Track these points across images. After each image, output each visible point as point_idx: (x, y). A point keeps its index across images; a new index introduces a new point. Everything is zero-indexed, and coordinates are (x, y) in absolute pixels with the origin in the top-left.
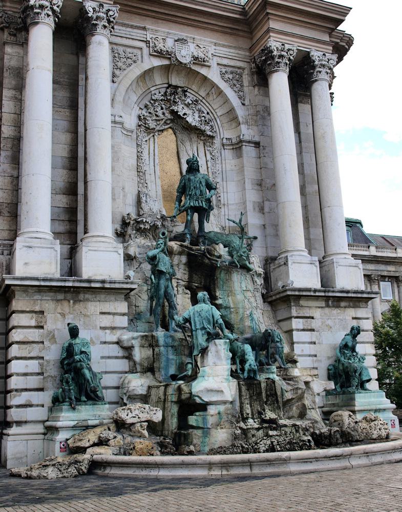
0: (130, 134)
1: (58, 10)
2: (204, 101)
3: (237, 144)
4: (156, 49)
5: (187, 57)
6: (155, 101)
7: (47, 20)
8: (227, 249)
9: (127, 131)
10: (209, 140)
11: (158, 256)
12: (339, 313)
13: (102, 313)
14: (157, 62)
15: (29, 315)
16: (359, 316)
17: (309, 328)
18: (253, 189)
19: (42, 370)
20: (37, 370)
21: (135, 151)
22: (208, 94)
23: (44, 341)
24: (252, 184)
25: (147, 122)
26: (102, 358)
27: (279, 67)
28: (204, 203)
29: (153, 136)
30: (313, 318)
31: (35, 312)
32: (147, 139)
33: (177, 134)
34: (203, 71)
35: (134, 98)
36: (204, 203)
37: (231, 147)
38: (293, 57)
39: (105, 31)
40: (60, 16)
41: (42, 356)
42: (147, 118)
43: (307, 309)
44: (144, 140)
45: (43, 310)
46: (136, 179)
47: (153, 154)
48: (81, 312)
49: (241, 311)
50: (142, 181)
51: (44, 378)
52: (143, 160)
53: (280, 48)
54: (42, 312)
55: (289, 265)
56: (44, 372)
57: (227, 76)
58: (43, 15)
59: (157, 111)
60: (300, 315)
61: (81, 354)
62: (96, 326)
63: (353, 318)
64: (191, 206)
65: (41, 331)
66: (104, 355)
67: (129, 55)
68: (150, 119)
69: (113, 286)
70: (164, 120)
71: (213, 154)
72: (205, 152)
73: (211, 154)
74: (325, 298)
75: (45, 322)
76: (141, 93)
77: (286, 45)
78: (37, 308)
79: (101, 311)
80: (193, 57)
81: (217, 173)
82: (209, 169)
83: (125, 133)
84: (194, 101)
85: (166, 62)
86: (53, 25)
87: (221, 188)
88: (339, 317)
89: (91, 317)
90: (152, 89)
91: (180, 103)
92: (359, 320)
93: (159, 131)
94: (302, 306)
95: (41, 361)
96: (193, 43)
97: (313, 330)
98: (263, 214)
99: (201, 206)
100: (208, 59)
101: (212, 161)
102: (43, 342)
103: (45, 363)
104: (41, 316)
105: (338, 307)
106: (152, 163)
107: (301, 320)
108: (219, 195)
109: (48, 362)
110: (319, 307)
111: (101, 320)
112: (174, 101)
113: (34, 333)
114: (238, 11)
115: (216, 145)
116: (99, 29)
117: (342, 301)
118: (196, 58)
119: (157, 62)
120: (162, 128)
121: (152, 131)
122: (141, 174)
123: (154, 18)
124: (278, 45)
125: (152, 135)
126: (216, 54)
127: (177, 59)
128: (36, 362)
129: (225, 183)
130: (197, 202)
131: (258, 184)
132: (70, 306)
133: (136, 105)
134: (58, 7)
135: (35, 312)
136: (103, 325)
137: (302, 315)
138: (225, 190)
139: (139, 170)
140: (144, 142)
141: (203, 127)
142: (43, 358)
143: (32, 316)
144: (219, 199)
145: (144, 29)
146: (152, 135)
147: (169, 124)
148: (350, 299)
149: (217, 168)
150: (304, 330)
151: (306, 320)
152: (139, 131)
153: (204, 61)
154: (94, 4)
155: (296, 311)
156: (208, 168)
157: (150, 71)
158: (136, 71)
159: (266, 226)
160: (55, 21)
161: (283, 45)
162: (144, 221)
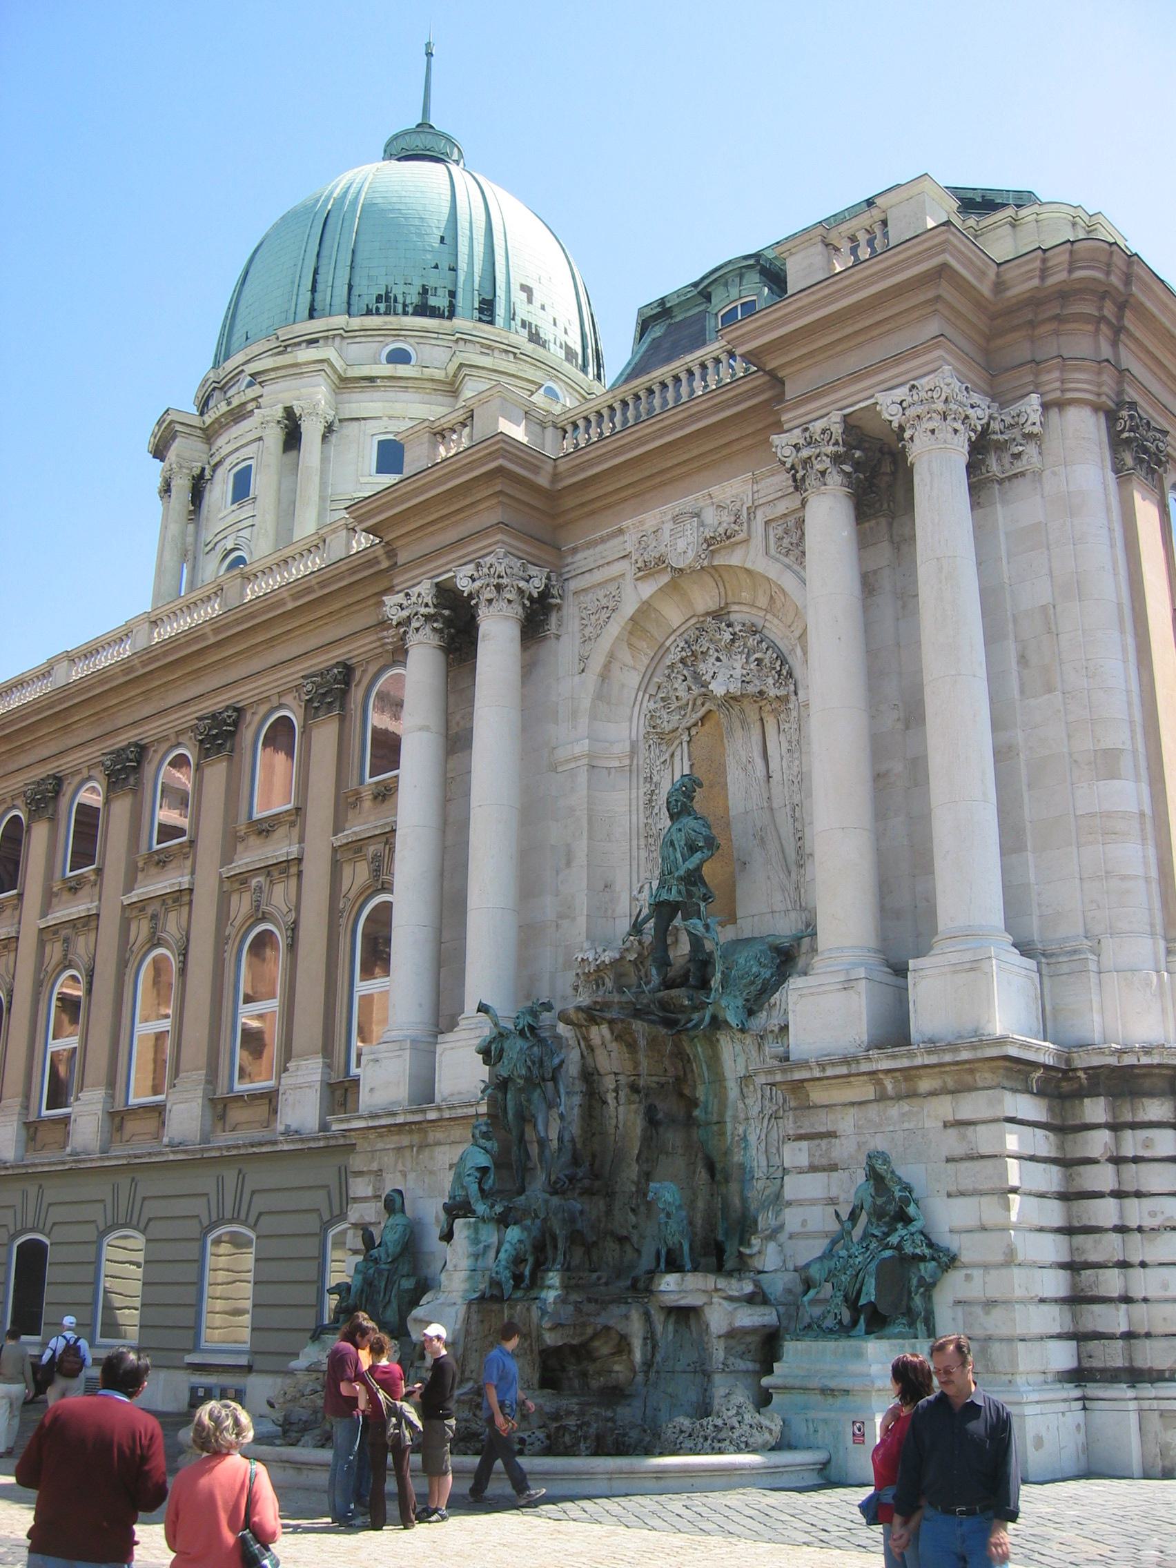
1: (431, 610)
2: (769, 617)
4: (638, 565)
5: (689, 551)
6: (672, 666)
7: (419, 637)
11: (493, 1048)
12: (904, 1115)
14: (648, 589)
16: (965, 1114)
17: (824, 1161)
22: (772, 596)
25: (659, 721)
27: (806, 490)
30: (831, 1135)
32: (667, 756)
34: (735, 559)
35: (633, 679)
38: (836, 443)
39: (491, 608)
40: (446, 612)
42: (658, 714)
43: (822, 1113)
44: (658, 763)
49: (729, 1127)
50: (655, 855)
52: (656, 810)
53: (802, 441)
57: (786, 542)
58: (411, 632)
59: (676, 689)
60: (802, 1131)
63: (946, 1125)
67: (604, 602)
68: (664, 713)
69: (454, 1114)
70: (691, 703)
74: (865, 1078)
76: (646, 662)
77: (810, 426)
78: (375, 1167)
80: (706, 540)
83: (617, 764)
84: (740, 631)
85: (665, 579)
86: (434, 640)
88: (906, 1126)
90: (668, 643)
91: (711, 652)
92: (962, 1129)
93: (689, 729)
94: (816, 1107)
96: (713, 504)
97: (833, 1168)
100: (737, 528)
105: (913, 1095)
107: (804, 1144)
108: (800, 835)
110: (853, 1104)
112: (702, 652)
114: (764, 383)
116: (483, 612)
117: (920, 1077)
118: (709, 542)
119: (648, 589)
120: (692, 721)
123: (636, 496)
124: (796, 436)
125: (677, 742)
126: (761, 501)
127: (672, 567)
133: (641, 694)
134: (427, 605)
137: (809, 1131)
141: (751, 689)
144: (799, 844)
145: (621, 531)
146: (677, 742)
147: (703, 705)
148: (937, 1070)
150: (813, 1169)
151: (817, 1142)
153: (728, 538)
154: (469, 569)
155: (795, 1122)
157: (646, 609)
158: (614, 629)
160: (434, 629)
161: (806, 430)
162: (579, 959)
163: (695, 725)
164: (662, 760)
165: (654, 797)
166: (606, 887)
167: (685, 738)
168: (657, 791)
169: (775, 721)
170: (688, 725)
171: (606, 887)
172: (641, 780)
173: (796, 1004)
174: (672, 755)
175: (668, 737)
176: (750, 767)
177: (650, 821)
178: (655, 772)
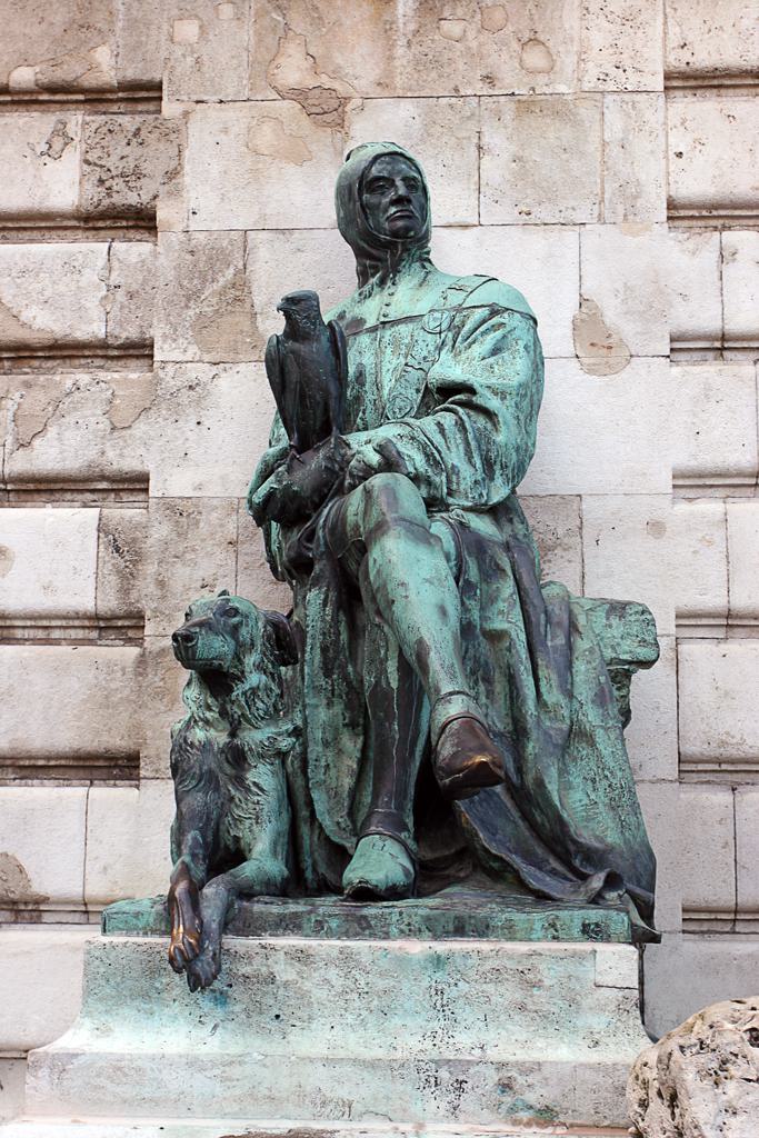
13: (691, 81)
15: (36, 125)
19: (125, 591)
20: (82, 592)
23: (156, 333)
26: (692, 482)
31: (96, 98)
41: (129, 464)
45: (157, 77)
48: (489, 79)
51: (142, 661)
54: (144, 93)
56: (148, 608)
61: (425, 409)
62: (631, 197)
65: (132, 250)
66: (709, 459)
75: (173, 174)
79: (678, 60)
89: (586, 112)
95: (125, 513)
102: (139, 350)
103: (160, 531)
104: (128, 122)
109: (181, 513)
111: (678, 142)
113: (72, 268)
128: (74, 521)
132: (388, 30)
135: (96, 98)
136: (696, 184)
142: (134, 484)
143: (61, 131)
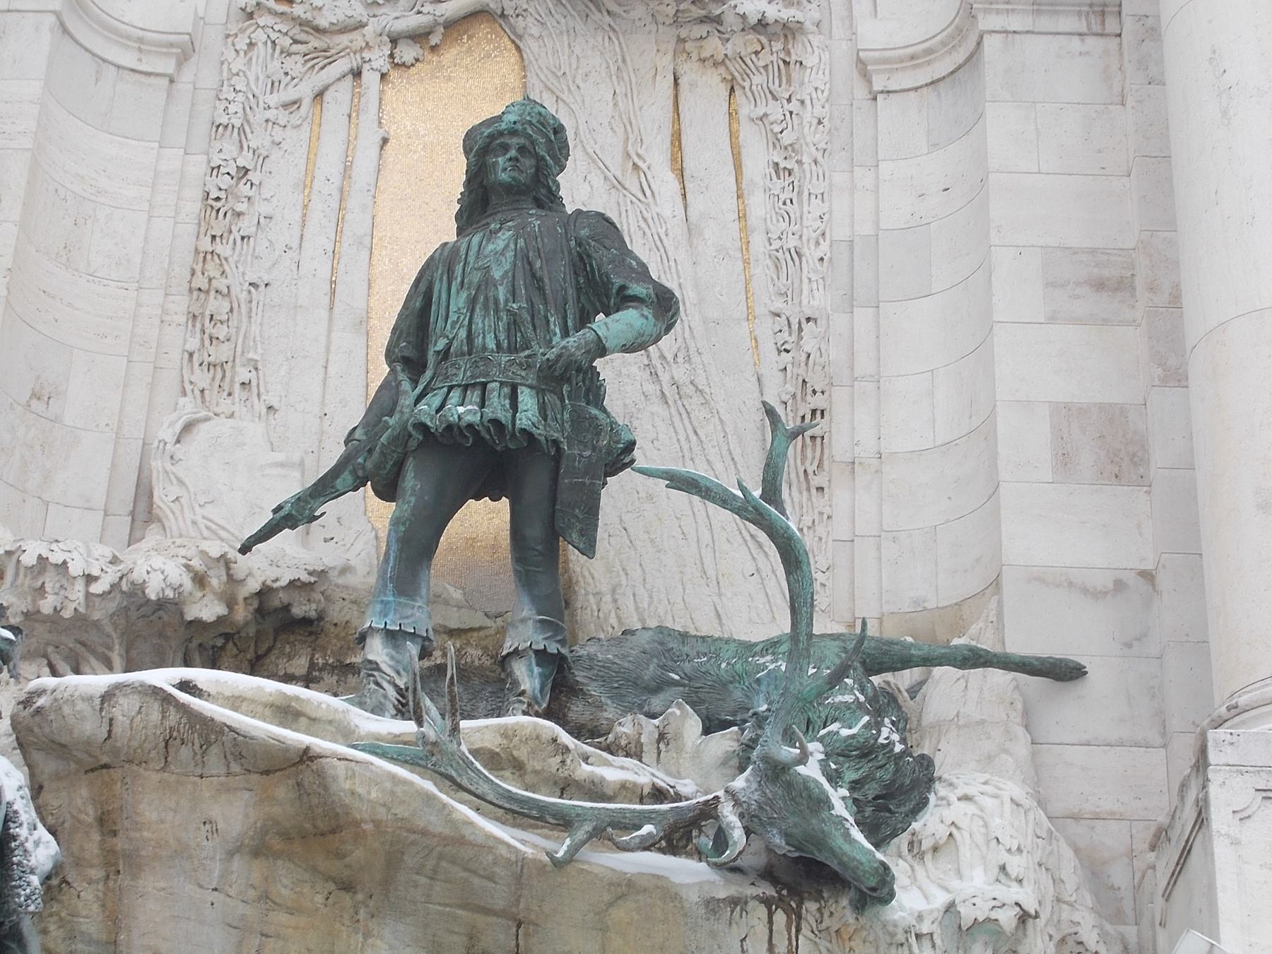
0: (167, 65)
3: (959, 34)
8: (725, 742)
9: (141, 44)
10: (766, 57)
18: (1052, 319)
21: (197, 166)
24: (1051, 285)
28: (527, 400)
29: (357, 74)
32: (305, 90)
33: (530, 46)
36: (527, 400)
37: (923, 76)
44: (273, 100)
46: (180, 338)
47: (336, 180)
52: (247, 226)
55: (1219, 818)
64: (422, 427)
71: (787, 138)
72: (733, 135)
73: (775, 141)
81: (811, 254)
82: (758, 241)
83: (128, 59)
87: (835, 353)
98: (1142, 481)
99: (496, 422)
101: (778, 185)
106: (318, 239)
108: (818, 402)
115: (819, 79)
120: (412, 22)
121: (344, 40)
122: (217, 305)
125: (342, 66)
129: (863, 317)
130: (475, 396)
131: (1100, 285)
138: (864, 365)
139: (200, 281)
140: (283, 117)
149: (811, 222)
152: (242, 44)
156: (745, 230)
159: (1163, 581)
162: (29, 559)
163: (419, 37)
164: (290, 94)
165: (244, 189)
166: (36, 396)
167: (378, 57)
168: (250, 176)
169: (723, 90)
170: (401, 26)
171: (36, 396)
172: (203, 127)
173: (1244, 817)
174: (319, 95)
175: (315, 42)
176: (632, 183)
177: (219, 248)
178: (258, 117)
